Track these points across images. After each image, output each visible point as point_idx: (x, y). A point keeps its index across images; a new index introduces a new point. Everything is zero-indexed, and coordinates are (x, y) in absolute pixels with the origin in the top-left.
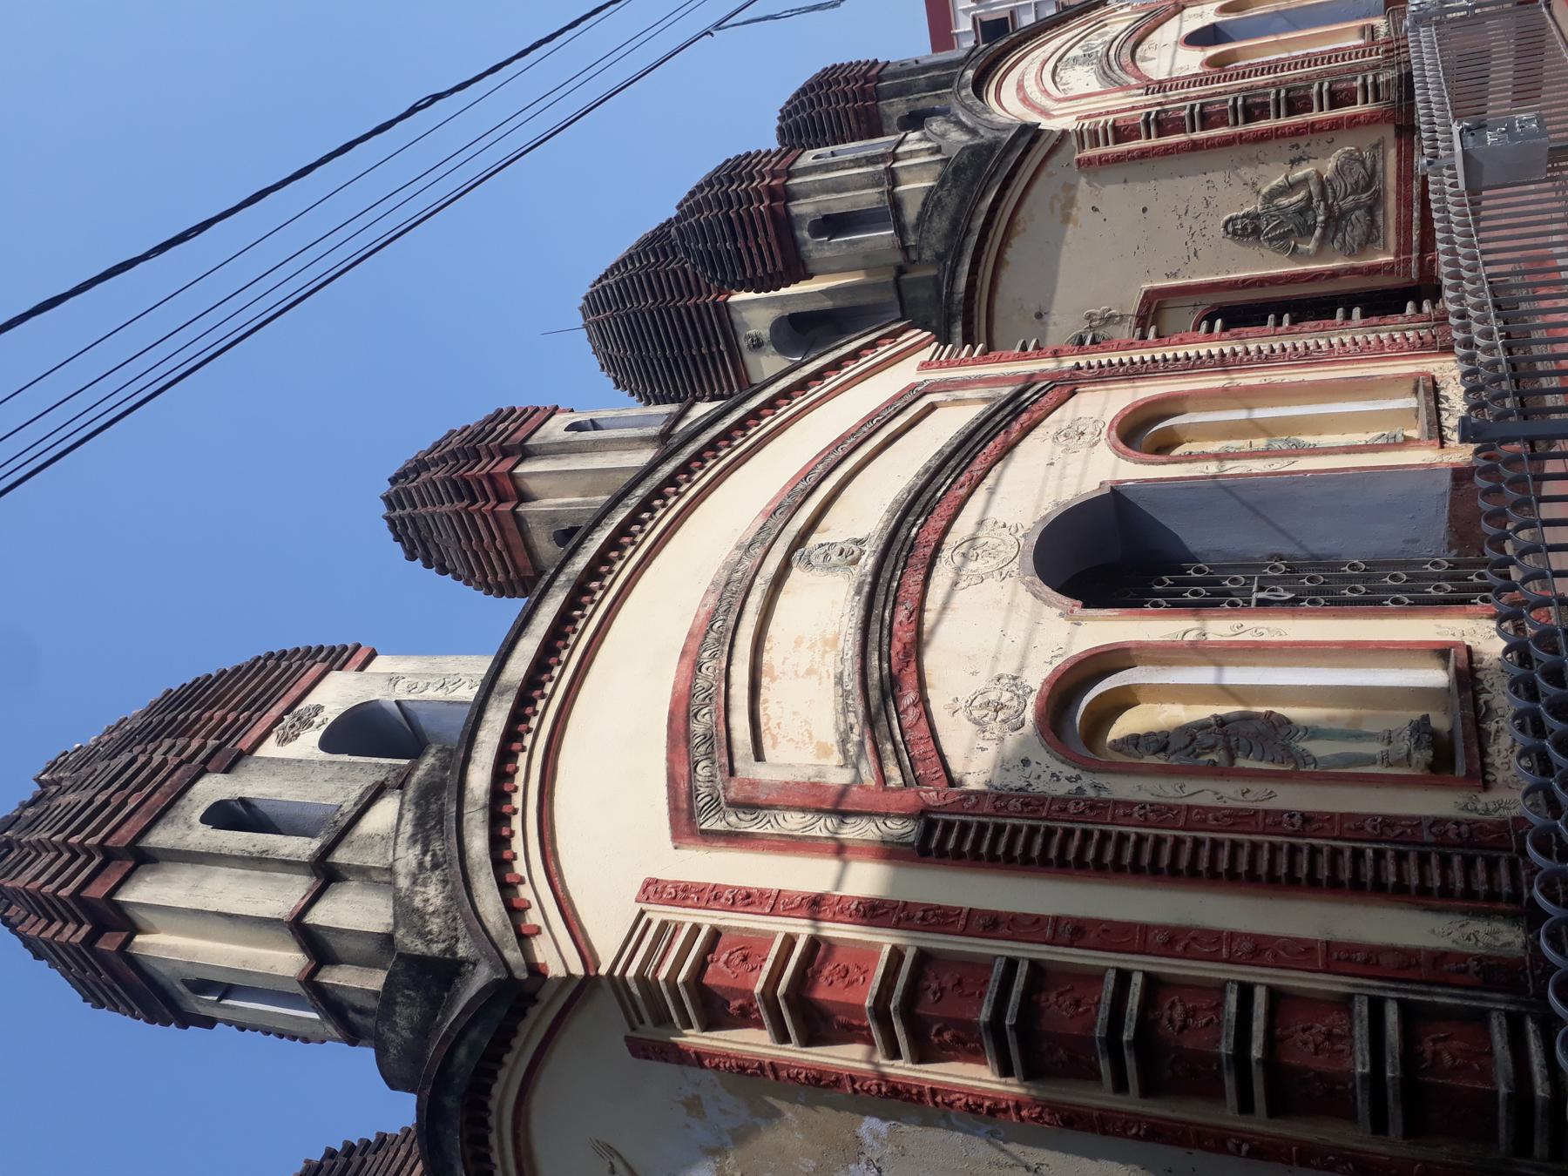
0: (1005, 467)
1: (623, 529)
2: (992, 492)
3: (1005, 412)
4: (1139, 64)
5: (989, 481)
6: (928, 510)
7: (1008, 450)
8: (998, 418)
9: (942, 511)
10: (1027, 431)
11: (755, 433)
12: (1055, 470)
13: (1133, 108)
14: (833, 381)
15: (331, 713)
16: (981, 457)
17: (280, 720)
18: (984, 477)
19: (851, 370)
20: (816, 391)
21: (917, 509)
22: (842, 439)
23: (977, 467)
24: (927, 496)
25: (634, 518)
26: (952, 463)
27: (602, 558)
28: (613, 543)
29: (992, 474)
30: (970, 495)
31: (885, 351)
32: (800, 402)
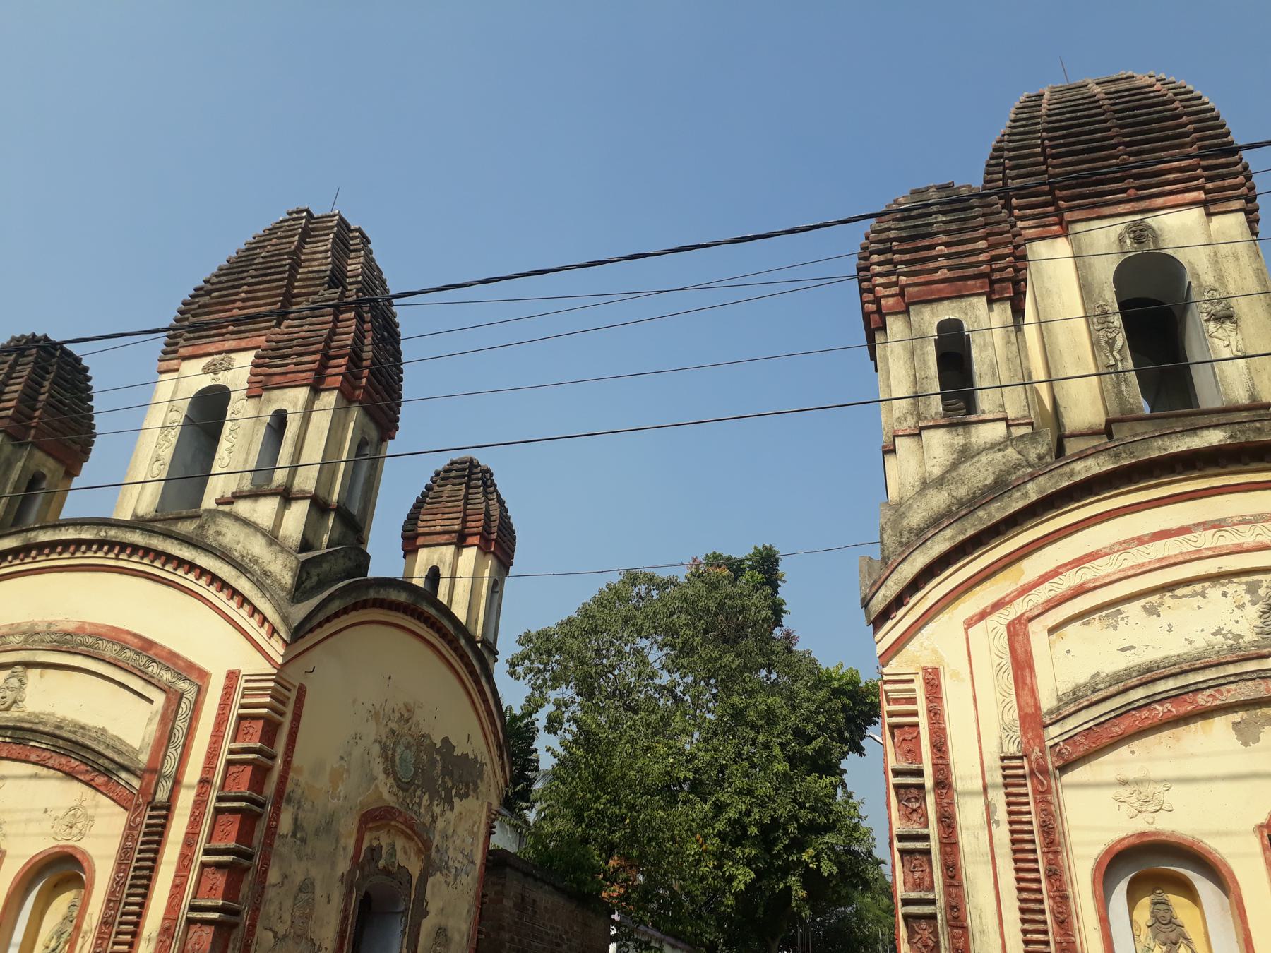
0: (58, 778)
1: (78, 543)
2: (36, 776)
3: (106, 763)
4: (1221, 724)
5: (45, 771)
6: (16, 740)
7: (71, 775)
8: (101, 761)
9: (16, 749)
10: (88, 784)
11: (180, 577)
12: (40, 814)
13: (940, 748)
14: (230, 607)
15: (224, 379)
16: (63, 760)
17: (220, 353)
18: (49, 768)
19: (241, 616)
20: (220, 599)
21: (19, 734)
22: (147, 645)
23: (56, 760)
24: (29, 736)
25: (89, 543)
26: (61, 742)
27: (52, 545)
28: (66, 544)
29: (52, 772)
30: (35, 763)
31: (260, 634)
32: (210, 593)
